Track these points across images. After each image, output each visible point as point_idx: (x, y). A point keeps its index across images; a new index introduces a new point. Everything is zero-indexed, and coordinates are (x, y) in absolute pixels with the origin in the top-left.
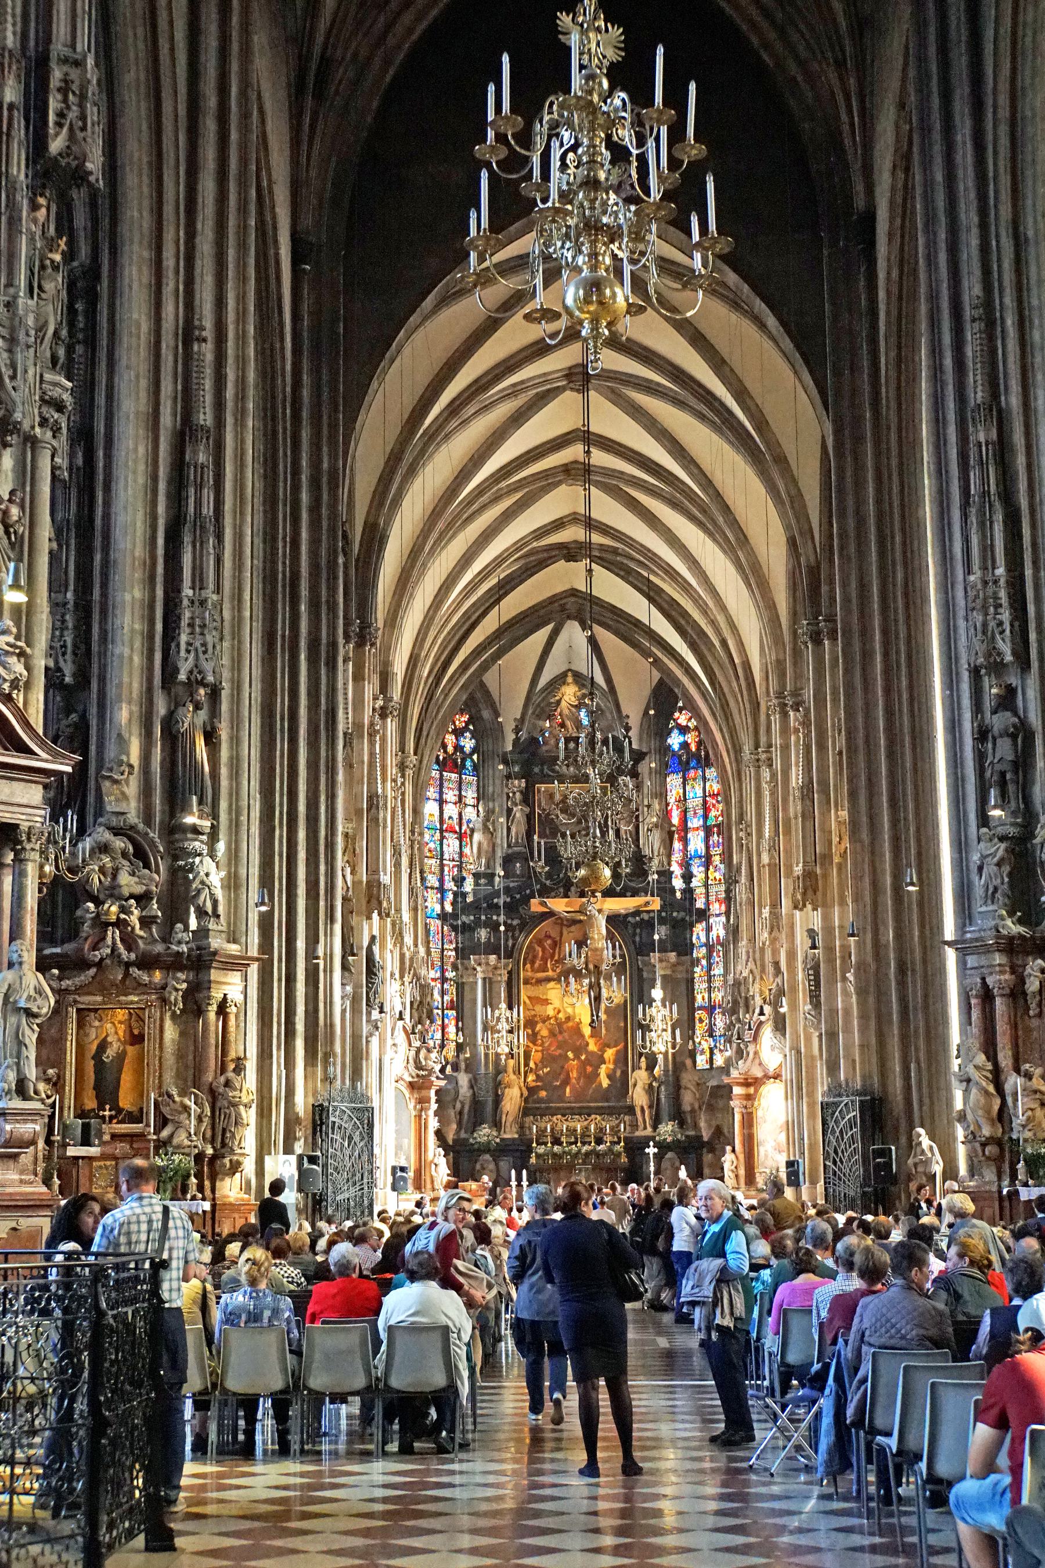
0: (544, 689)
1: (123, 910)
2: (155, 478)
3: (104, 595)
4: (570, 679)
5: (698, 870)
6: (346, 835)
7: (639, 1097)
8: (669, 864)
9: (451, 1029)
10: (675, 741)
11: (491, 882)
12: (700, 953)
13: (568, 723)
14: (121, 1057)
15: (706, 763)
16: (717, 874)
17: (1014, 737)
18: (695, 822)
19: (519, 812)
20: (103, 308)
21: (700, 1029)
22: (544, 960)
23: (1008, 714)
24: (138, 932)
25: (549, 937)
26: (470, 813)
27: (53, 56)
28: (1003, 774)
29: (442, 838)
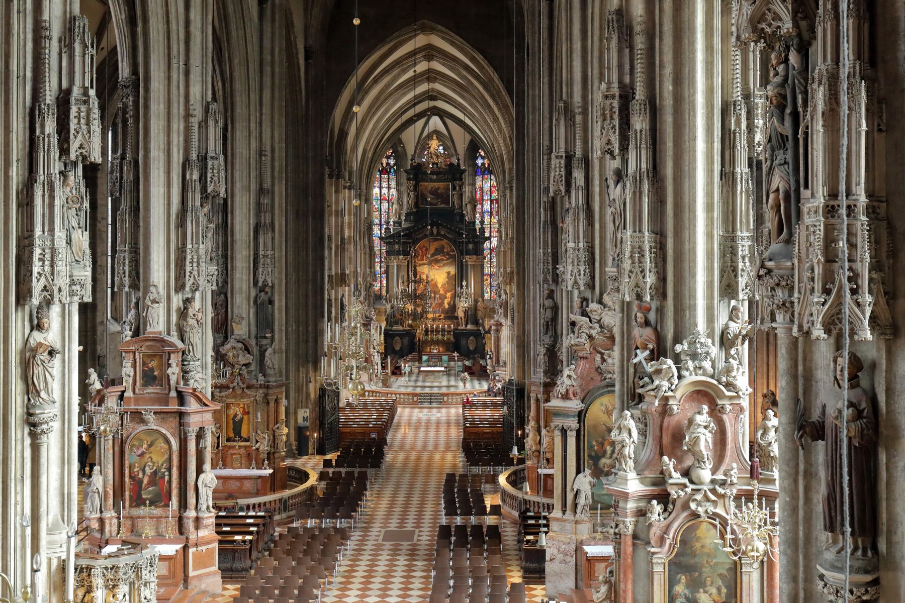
0: (425, 138)
1: (240, 369)
2: (250, 210)
3: (232, 253)
4: (435, 137)
5: (487, 218)
6: (329, 276)
7: (460, 313)
8: (475, 217)
9: (384, 282)
10: (479, 162)
11: (400, 226)
12: (487, 252)
13: (434, 156)
14: (242, 419)
15: (491, 173)
16: (495, 220)
17: (552, 310)
18: (486, 197)
19: (412, 194)
20: (229, 141)
21: (486, 283)
22: (422, 256)
23: (551, 300)
24: (247, 377)
25: (424, 246)
26: (393, 191)
27: (208, 157)
28: (548, 322)
29: (381, 203)
